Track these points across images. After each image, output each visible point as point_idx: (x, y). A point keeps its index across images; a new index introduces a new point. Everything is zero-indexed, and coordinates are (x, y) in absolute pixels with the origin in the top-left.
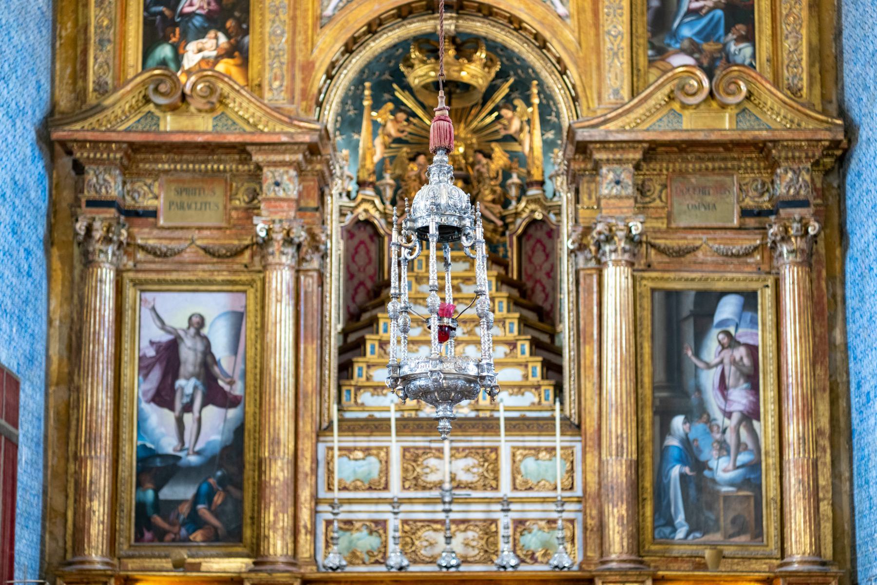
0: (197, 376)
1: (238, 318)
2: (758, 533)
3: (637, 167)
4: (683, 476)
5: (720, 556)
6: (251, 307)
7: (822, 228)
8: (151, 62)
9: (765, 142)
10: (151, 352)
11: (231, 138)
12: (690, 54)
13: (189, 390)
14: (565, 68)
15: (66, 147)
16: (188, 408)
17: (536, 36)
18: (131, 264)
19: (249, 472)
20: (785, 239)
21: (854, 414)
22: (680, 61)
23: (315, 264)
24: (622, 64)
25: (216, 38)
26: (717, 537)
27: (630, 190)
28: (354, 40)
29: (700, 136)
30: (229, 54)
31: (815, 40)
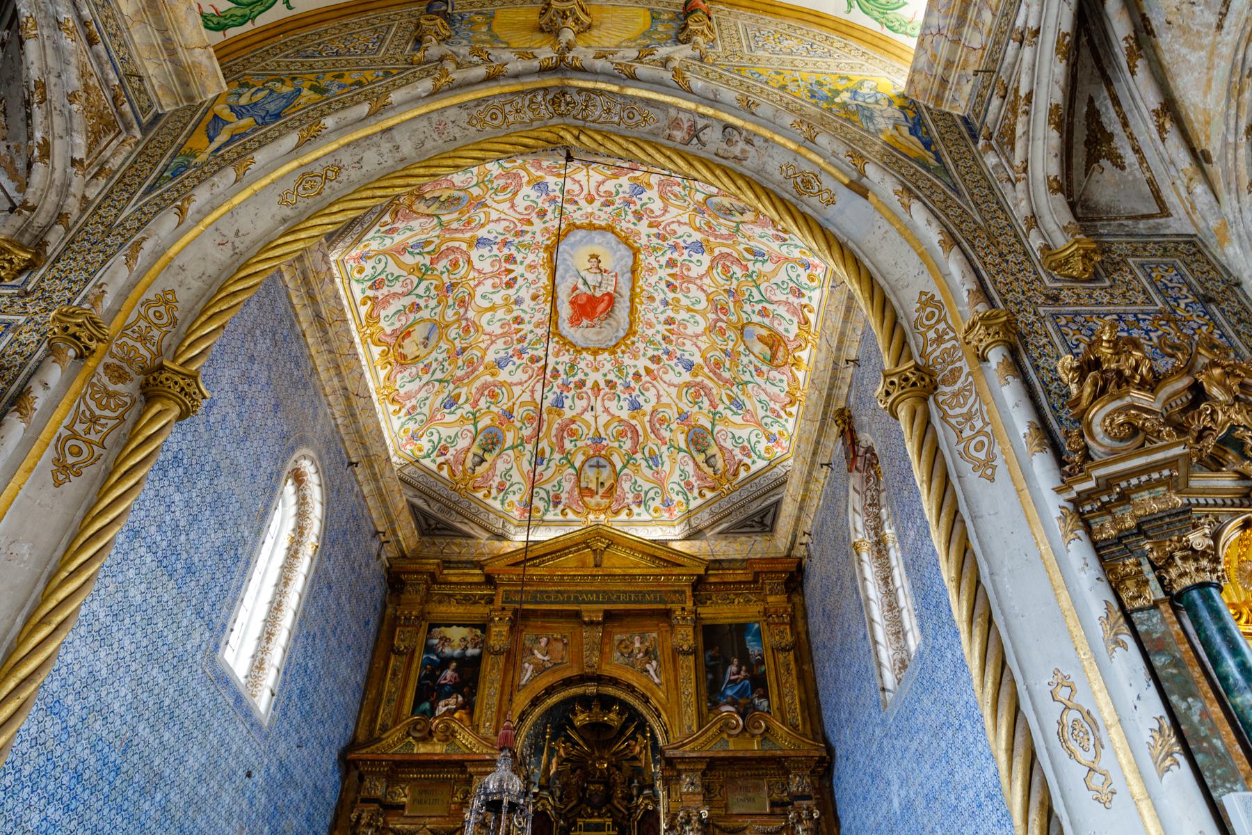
3: (704, 774)
7: (821, 814)
9: (780, 757)
11: (456, 757)
12: (732, 705)
17: (643, 695)
20: (800, 821)
24: (692, 711)
27: (700, 789)
29: (740, 754)
31: (803, 697)
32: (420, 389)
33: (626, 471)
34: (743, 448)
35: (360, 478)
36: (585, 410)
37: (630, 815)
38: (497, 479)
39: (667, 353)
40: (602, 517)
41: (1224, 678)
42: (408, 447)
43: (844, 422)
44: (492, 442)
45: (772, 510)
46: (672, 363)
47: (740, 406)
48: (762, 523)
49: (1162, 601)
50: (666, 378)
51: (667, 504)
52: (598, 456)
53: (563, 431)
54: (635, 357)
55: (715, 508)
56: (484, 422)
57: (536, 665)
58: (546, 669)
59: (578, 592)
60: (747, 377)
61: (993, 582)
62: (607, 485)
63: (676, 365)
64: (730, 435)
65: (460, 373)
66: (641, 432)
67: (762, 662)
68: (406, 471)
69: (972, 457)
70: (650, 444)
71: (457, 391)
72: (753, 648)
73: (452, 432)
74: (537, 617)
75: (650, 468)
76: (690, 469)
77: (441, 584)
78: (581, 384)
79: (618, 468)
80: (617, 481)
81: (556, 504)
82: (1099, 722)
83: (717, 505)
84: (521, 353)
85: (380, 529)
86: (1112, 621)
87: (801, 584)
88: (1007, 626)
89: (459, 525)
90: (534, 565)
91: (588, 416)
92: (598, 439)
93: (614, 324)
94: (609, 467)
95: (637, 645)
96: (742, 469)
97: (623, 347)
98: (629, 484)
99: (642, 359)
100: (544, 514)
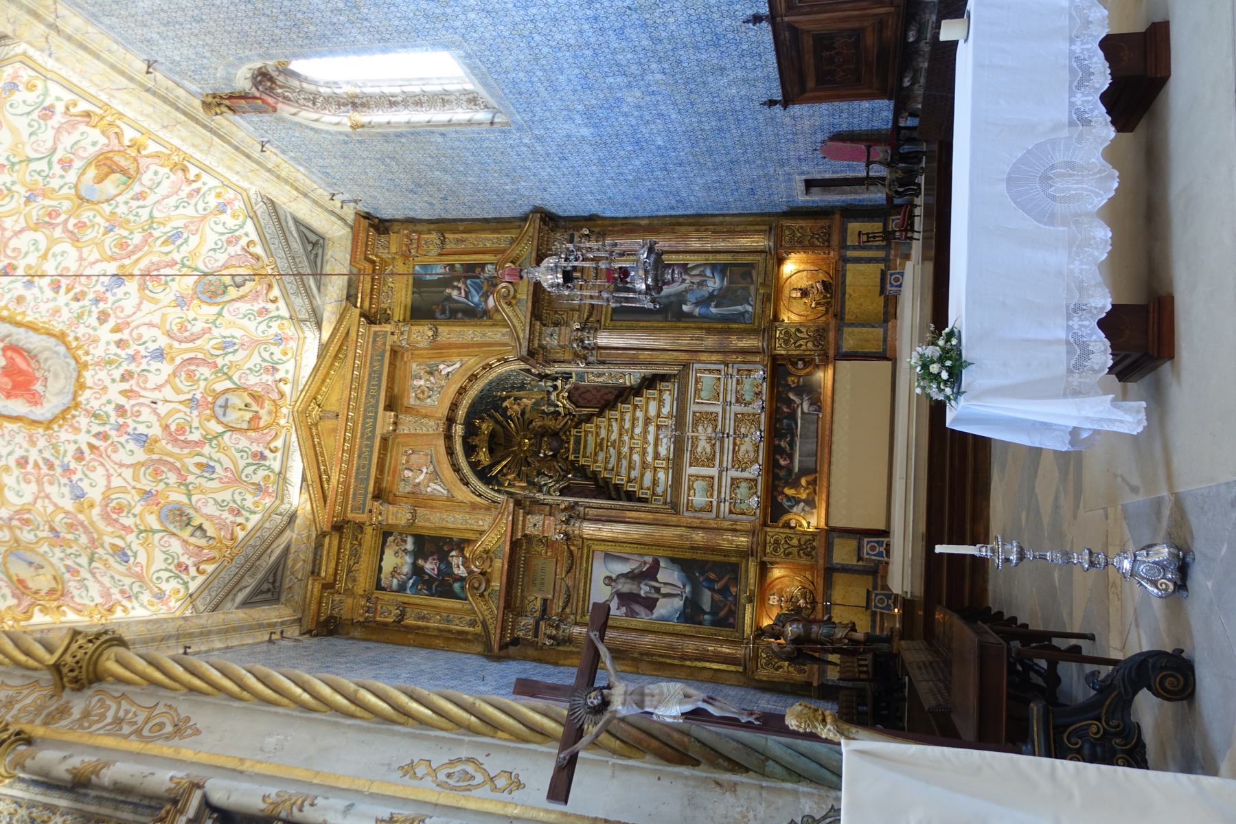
0: (640, 583)
1: (608, 556)
2: (751, 266)
3: (545, 325)
4: (716, 307)
5: (764, 284)
6: (602, 548)
8: (462, 595)
10: (624, 609)
12: (488, 297)
13: (647, 589)
14: (488, 364)
15: (504, 646)
16: (657, 590)
18: (572, 617)
19: (699, 556)
21: (688, 212)
22: (491, 302)
23: (581, 509)
25: (453, 556)
26: (752, 288)
27: (556, 328)
28: (461, 480)
30: (462, 550)
32: (99, 582)
33: (235, 378)
34: (229, 242)
35: (203, 648)
36: (155, 411)
37: (570, 414)
38: (225, 515)
39: (97, 301)
40: (284, 410)
42: (172, 604)
43: (219, 105)
44: (180, 517)
45: (302, 228)
46: (111, 299)
47: (178, 235)
48: (315, 244)
50: (128, 311)
51: (280, 340)
52: (216, 405)
53: (176, 440)
54: (96, 341)
55: (291, 288)
56: (153, 521)
57: (430, 480)
58: (435, 472)
59: (362, 437)
60: (144, 214)
62: (249, 400)
63: (114, 295)
64: (212, 253)
65: (84, 540)
66: (192, 355)
67: (452, 266)
68: (202, 608)
70: (208, 347)
71: (107, 546)
72: (439, 271)
73: (159, 558)
74: (382, 479)
75: (236, 351)
76: (243, 307)
77: (335, 580)
78: (121, 410)
79: (234, 386)
80: (245, 389)
81: (263, 457)
83: (288, 286)
84: (67, 470)
85: (267, 637)
87: (382, 221)
89: (273, 558)
90: (328, 480)
91: (163, 409)
92: (192, 403)
93: (46, 354)
94: (227, 396)
95: (422, 382)
96: (252, 249)
97: (80, 352)
98: (251, 377)
99: (98, 333)
100: (273, 471)
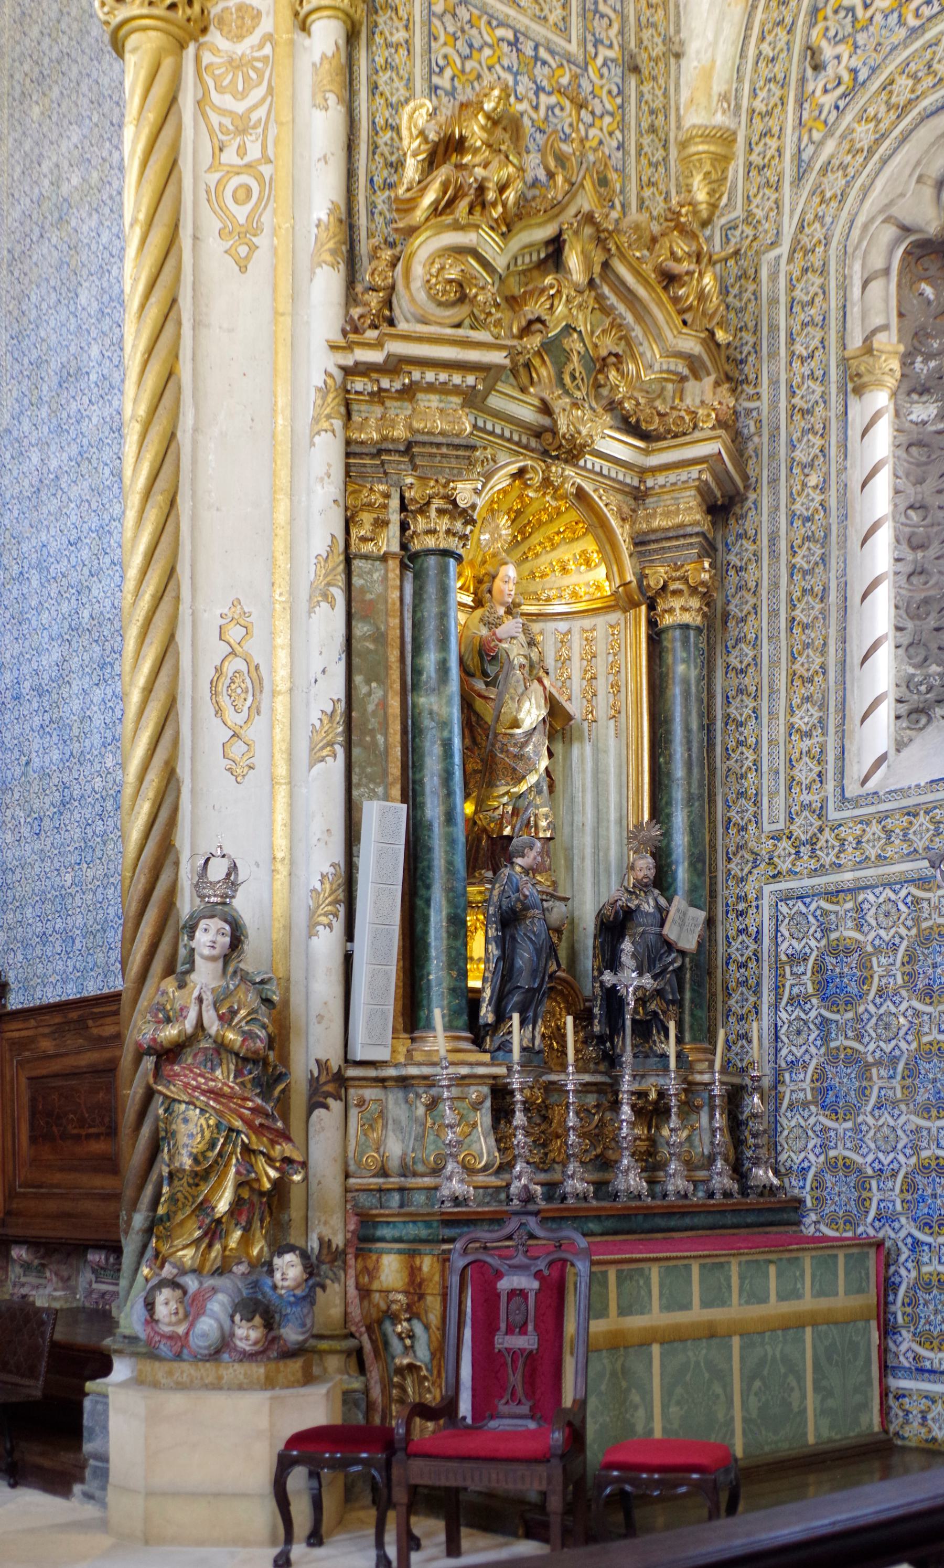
41: (417, 672)
49: (394, 555)
61: (195, 442)
69: (224, 208)
82: (266, 683)
86: (331, 565)
88: (194, 518)
